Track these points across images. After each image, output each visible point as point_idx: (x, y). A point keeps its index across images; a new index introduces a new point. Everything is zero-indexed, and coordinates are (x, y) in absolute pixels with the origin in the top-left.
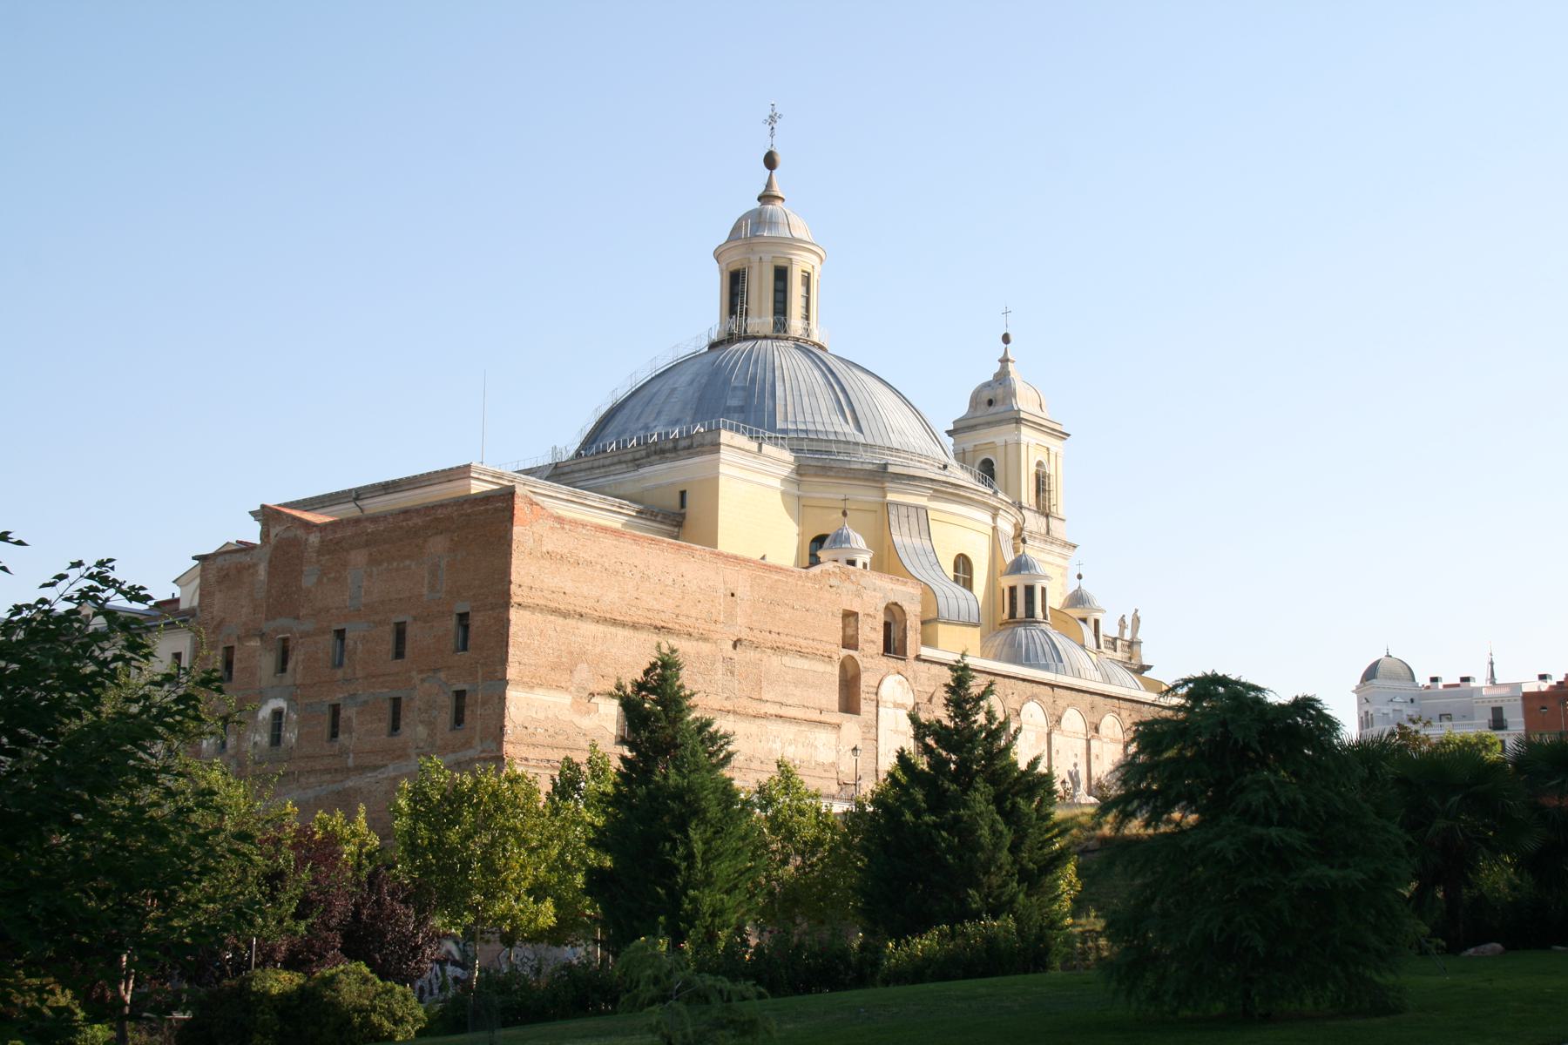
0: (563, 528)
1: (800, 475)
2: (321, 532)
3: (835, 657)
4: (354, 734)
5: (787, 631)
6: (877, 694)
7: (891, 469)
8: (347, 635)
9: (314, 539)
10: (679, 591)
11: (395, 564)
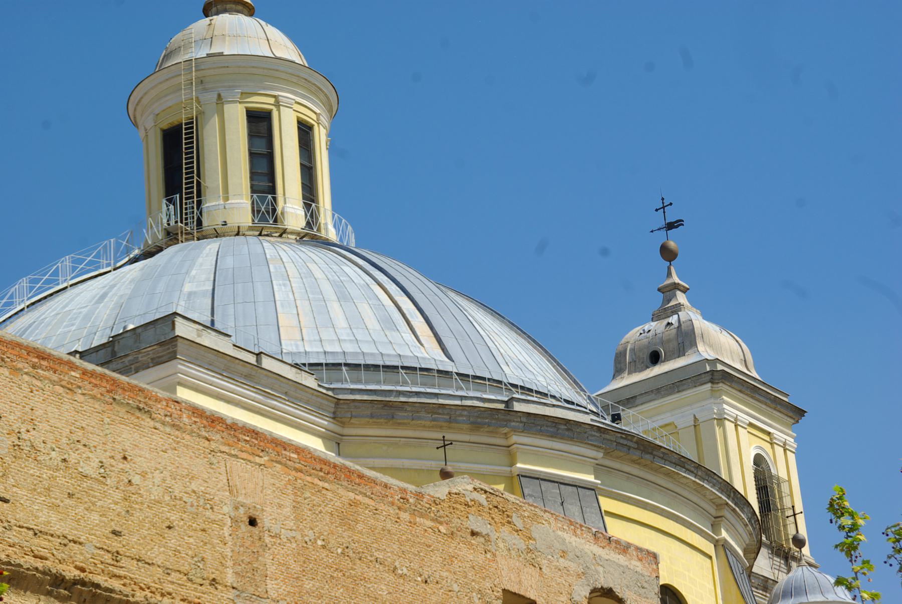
1: (343, 424)
7: (518, 407)
10: (118, 496)
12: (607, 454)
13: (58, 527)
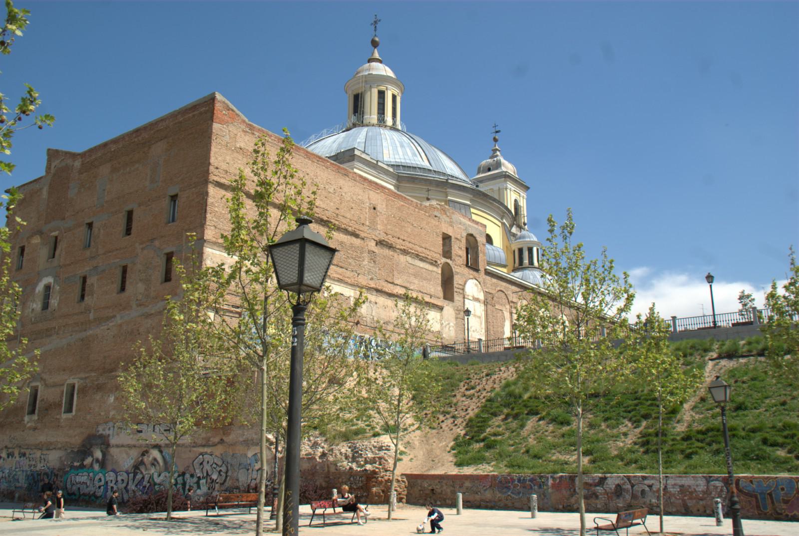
0: (253, 134)
1: (400, 182)
2: (82, 158)
3: (439, 263)
4: (95, 295)
5: (409, 240)
6: (463, 289)
7: (450, 181)
8: (94, 225)
9: (78, 164)
10: (338, 198)
11: (128, 169)
12: (474, 196)
13: (322, 206)
